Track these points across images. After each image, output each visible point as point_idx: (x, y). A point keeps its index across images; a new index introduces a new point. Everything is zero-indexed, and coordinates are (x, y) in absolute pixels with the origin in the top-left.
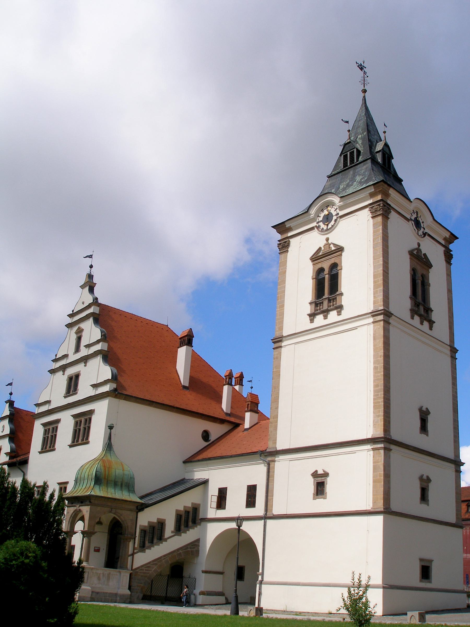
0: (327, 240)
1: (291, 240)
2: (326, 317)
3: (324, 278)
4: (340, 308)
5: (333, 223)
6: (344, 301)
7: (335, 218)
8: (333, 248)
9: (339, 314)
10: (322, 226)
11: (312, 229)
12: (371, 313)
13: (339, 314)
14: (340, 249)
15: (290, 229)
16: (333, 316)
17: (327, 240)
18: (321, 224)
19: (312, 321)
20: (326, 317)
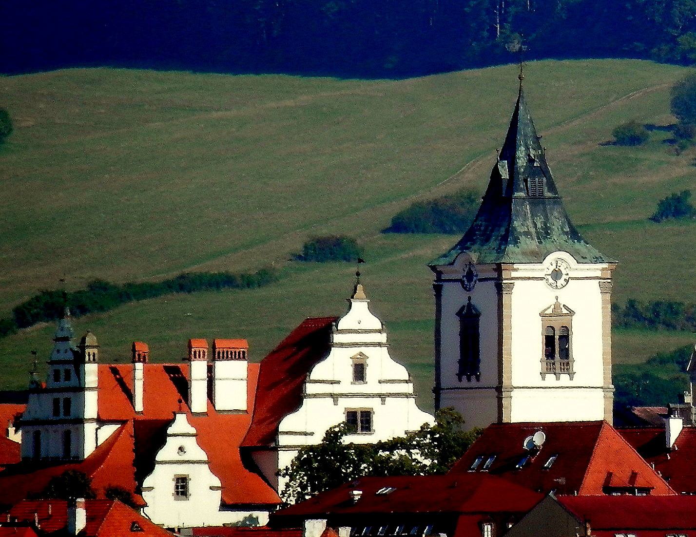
0: (557, 298)
1: (517, 282)
2: (558, 379)
3: (553, 337)
4: (571, 375)
5: (561, 282)
6: (576, 367)
7: (564, 277)
8: (565, 311)
9: (571, 379)
10: (551, 281)
11: (542, 279)
12: (602, 388)
13: (571, 379)
14: (571, 313)
15: (516, 270)
16: (564, 379)
17: (557, 298)
18: (549, 277)
19: (543, 379)
20: (558, 379)
